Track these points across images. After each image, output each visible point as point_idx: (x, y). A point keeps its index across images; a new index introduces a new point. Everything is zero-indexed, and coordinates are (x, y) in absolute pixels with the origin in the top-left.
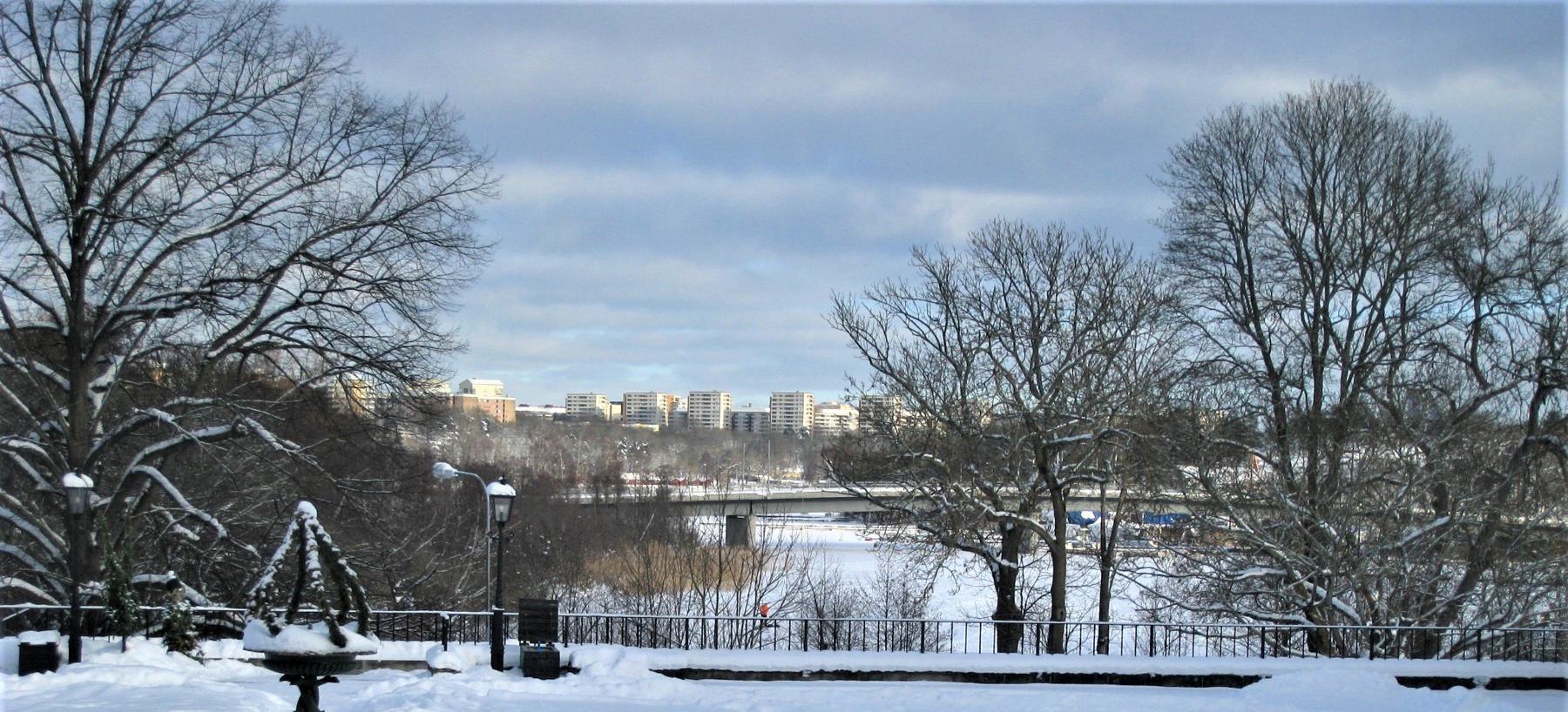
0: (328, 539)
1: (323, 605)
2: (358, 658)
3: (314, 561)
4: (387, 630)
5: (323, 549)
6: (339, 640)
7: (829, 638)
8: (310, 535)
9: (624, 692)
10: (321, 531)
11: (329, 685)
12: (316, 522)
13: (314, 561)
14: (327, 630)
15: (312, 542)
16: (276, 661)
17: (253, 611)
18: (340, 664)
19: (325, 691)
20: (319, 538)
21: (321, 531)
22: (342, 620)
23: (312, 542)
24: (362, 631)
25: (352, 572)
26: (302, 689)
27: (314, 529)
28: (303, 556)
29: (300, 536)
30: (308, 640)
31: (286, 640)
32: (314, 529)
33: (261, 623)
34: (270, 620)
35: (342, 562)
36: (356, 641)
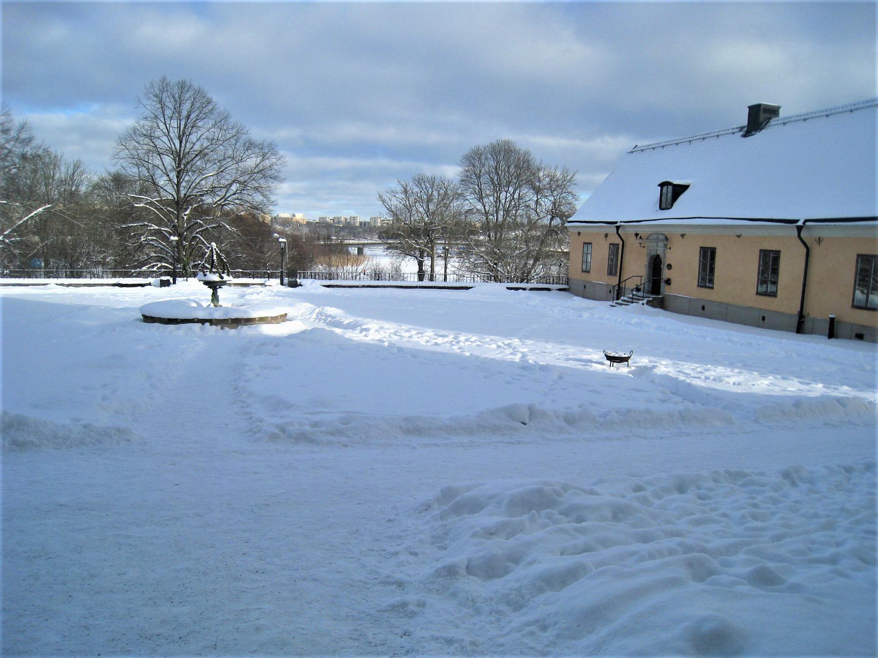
0: (219, 252)
1: (217, 269)
2: (227, 282)
3: (215, 258)
4: (237, 276)
5: (217, 254)
6: (222, 278)
7: (317, 277)
8: (214, 251)
9: (312, 291)
10: (217, 250)
11: (220, 289)
12: (216, 248)
13: (215, 258)
14: (218, 275)
15: (215, 253)
16: (206, 283)
17: (200, 270)
18: (224, 283)
19: (219, 290)
20: (216, 252)
21: (217, 250)
22: (223, 273)
23: (215, 253)
24: (228, 275)
25: (225, 260)
26: (213, 290)
27: (215, 249)
28: (213, 256)
29: (212, 251)
30: (215, 278)
31: (208, 278)
32: (215, 249)
33: (202, 273)
34: (204, 272)
35: (223, 258)
36: (226, 277)
